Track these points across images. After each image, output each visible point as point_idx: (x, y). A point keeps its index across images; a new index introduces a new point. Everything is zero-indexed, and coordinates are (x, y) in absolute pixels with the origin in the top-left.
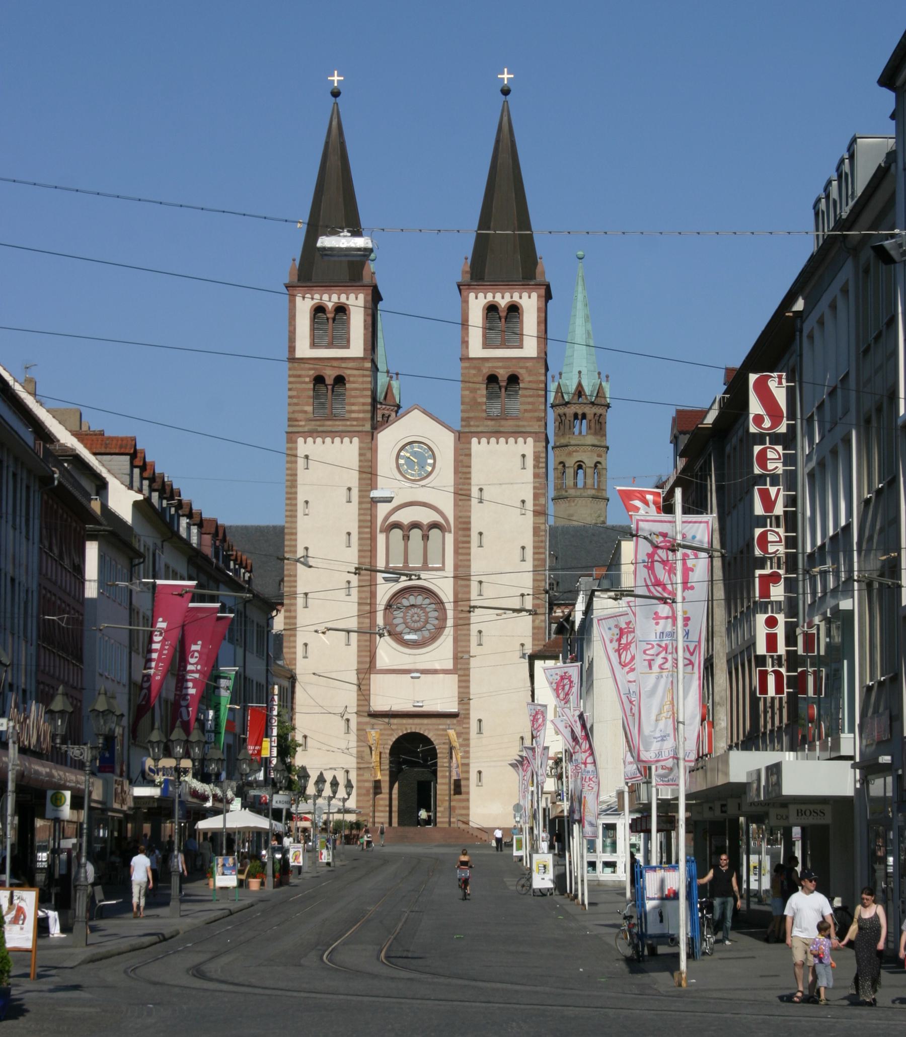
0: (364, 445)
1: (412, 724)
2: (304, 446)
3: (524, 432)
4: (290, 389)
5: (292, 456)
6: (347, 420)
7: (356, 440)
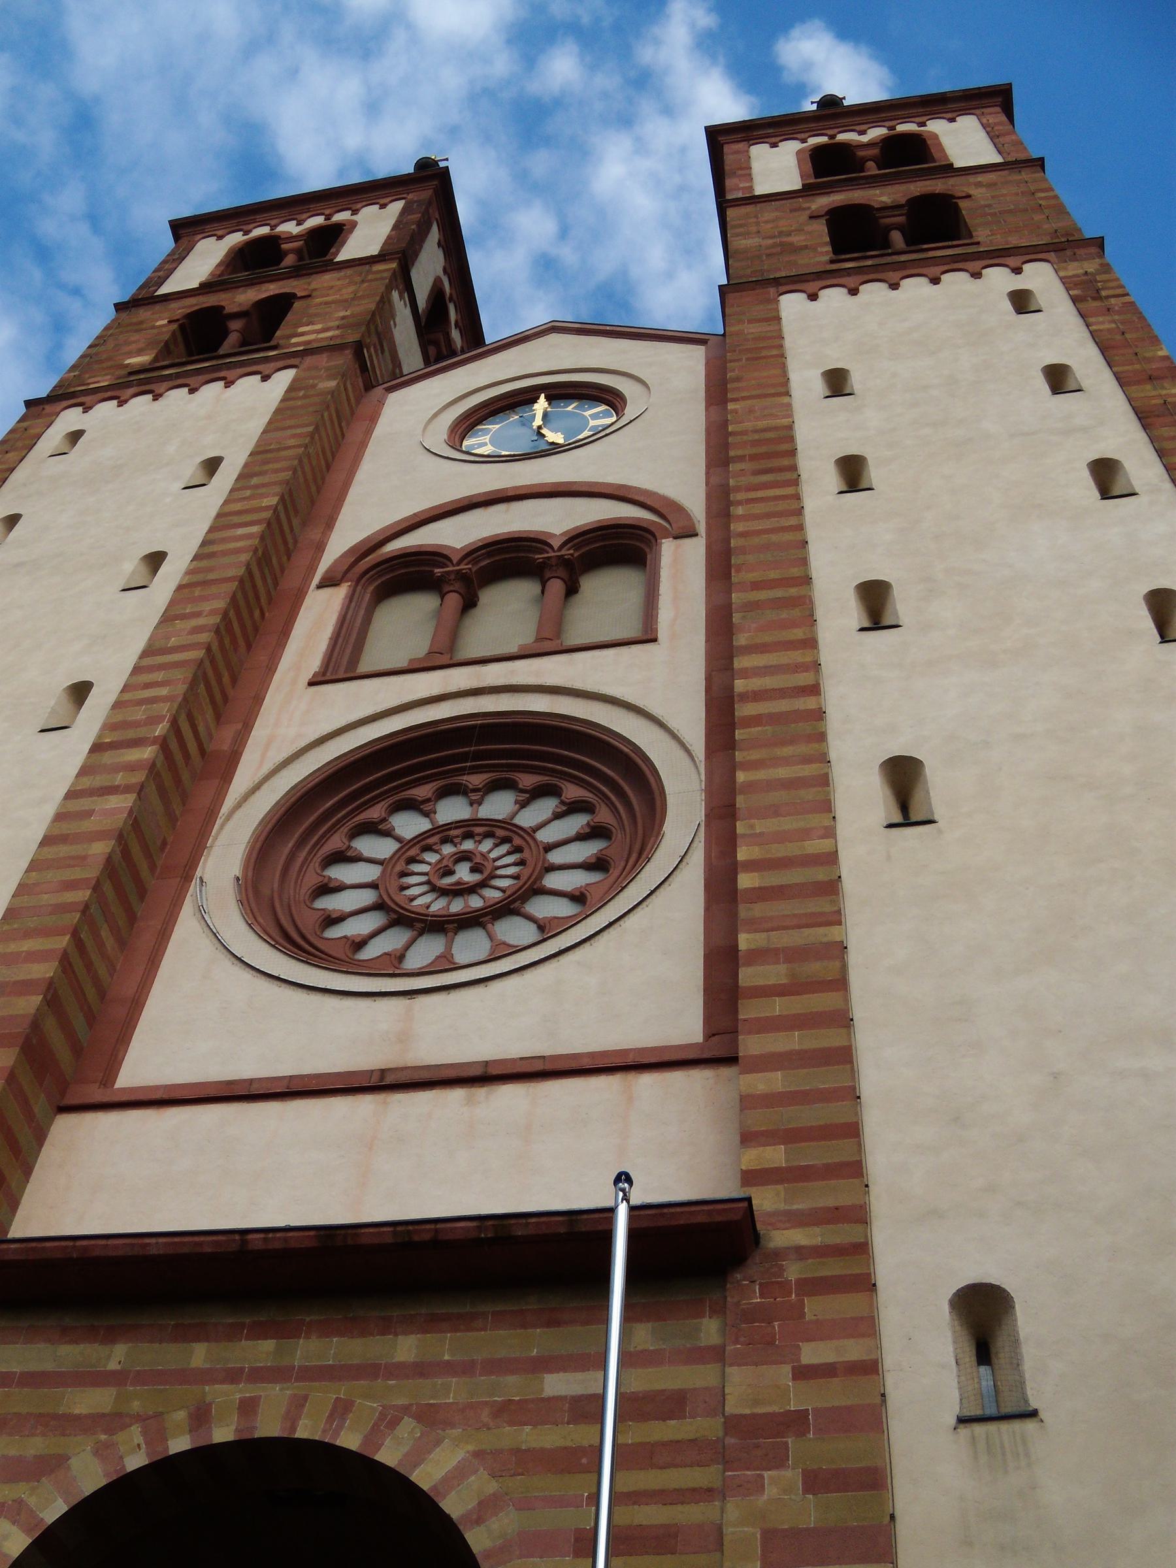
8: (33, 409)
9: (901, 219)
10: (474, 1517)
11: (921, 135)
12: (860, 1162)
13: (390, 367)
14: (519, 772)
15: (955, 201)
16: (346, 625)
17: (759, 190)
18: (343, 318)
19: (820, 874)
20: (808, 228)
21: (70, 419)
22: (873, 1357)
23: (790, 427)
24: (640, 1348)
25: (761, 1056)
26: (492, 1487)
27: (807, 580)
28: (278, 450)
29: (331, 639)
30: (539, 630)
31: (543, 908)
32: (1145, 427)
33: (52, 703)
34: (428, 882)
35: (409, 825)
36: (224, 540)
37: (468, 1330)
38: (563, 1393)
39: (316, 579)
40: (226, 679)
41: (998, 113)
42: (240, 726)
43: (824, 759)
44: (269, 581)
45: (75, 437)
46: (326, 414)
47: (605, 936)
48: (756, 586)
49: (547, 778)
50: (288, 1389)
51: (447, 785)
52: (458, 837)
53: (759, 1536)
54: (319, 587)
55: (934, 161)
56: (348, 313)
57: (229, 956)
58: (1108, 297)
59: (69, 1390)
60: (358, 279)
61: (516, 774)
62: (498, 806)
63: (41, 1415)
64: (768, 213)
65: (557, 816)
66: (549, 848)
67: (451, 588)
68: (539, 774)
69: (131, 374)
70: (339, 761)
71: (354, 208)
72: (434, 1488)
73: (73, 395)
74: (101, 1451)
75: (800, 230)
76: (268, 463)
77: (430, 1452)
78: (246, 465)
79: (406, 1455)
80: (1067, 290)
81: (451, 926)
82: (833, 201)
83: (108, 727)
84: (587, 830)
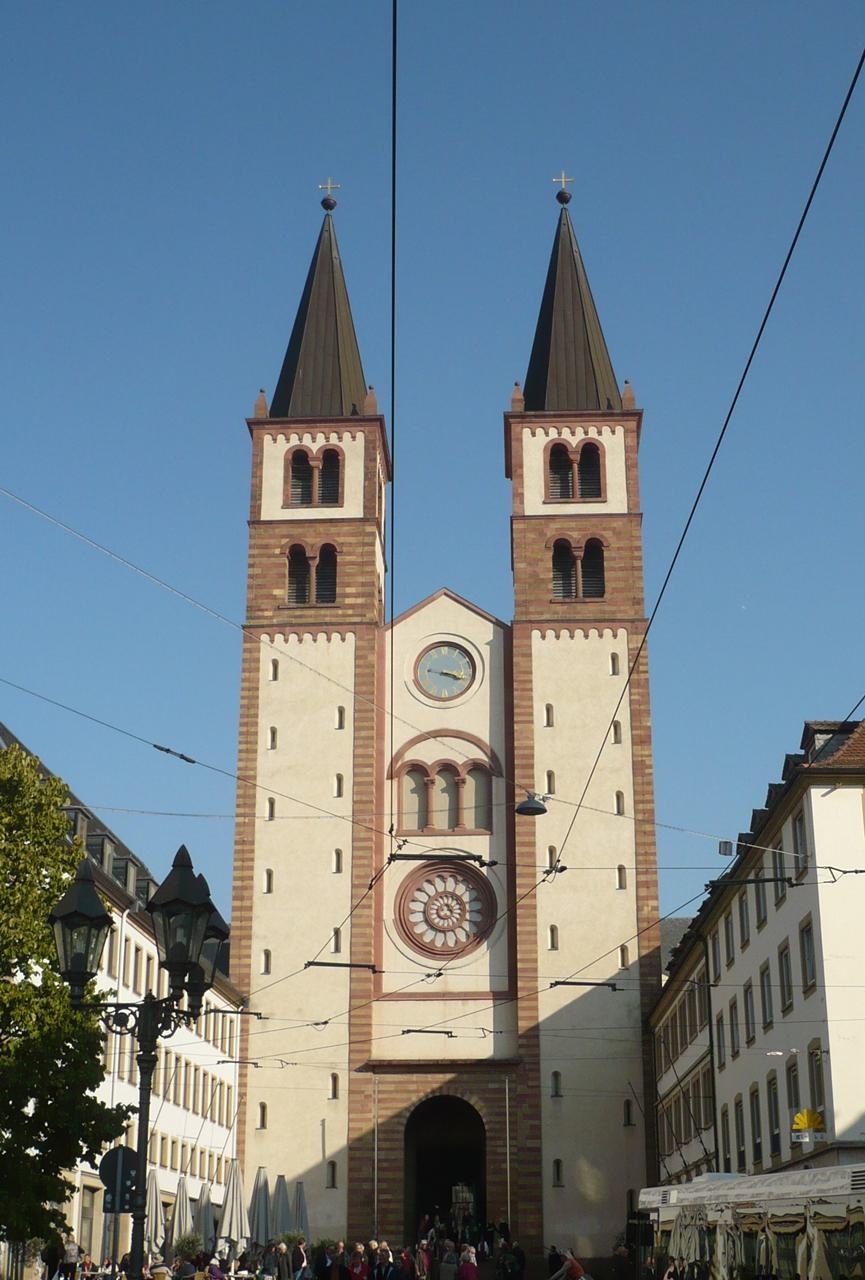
0: (360, 643)
2: (270, 649)
3: (613, 621)
4: (251, 566)
5: (251, 664)
7: (350, 636)
17: (526, 514)
18: (363, 584)
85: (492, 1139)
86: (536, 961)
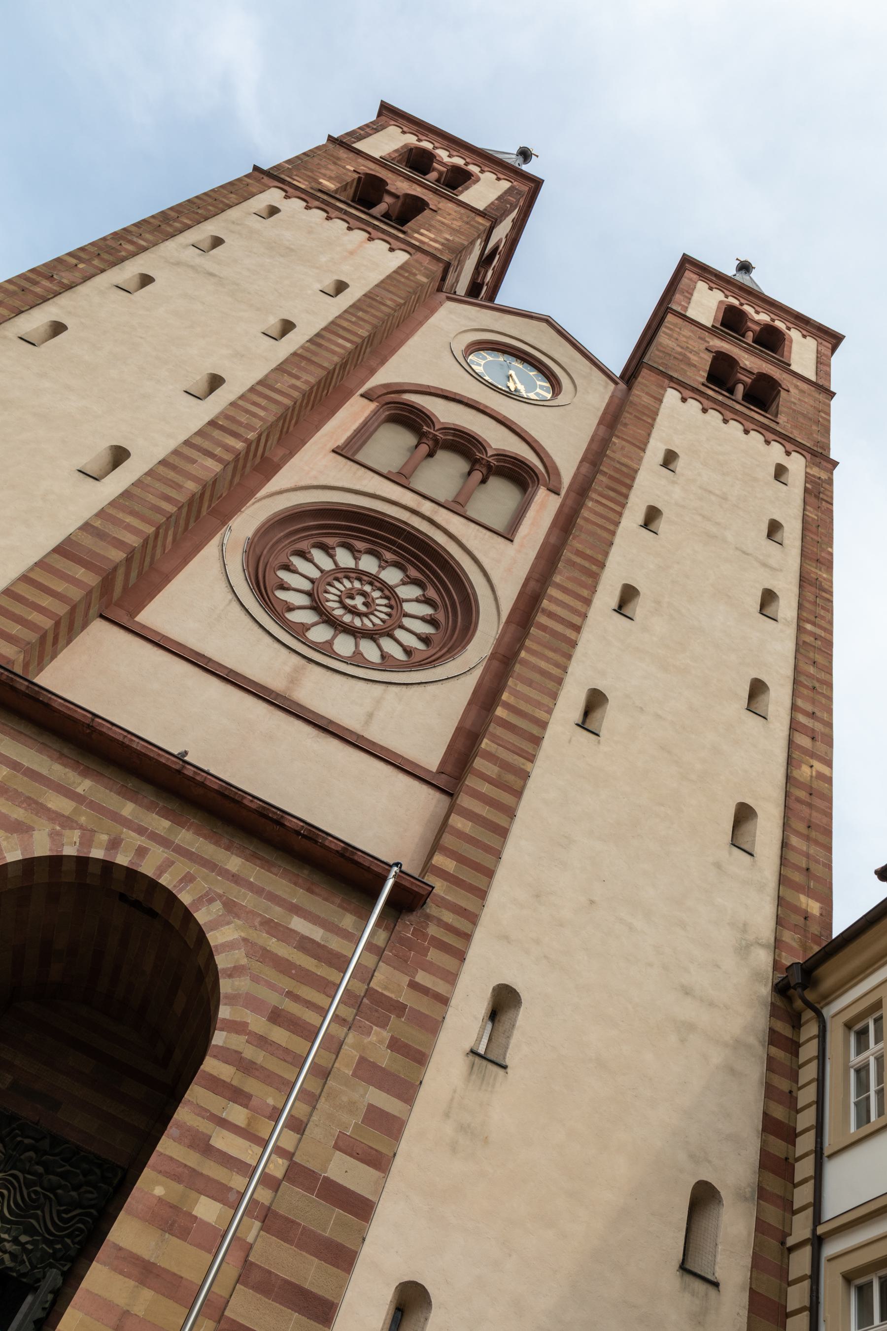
1: (154, 837)
6: (404, 232)
8: (257, 173)
9: (749, 381)
10: (229, 973)
11: (784, 335)
12: (487, 892)
13: (454, 281)
14: (412, 566)
15: (780, 388)
16: (365, 428)
18: (448, 240)
19: (535, 730)
20: (702, 355)
21: (273, 196)
22: (448, 996)
23: (636, 471)
24: (344, 927)
25: (466, 809)
26: (244, 961)
27: (602, 565)
28: (381, 303)
29: (355, 431)
30: (458, 495)
31: (388, 645)
32: (801, 586)
33: (198, 378)
34: (339, 596)
35: (344, 559)
36: (329, 340)
37: (268, 871)
38: (299, 931)
39: (362, 390)
40: (293, 422)
41: (829, 348)
42: (287, 452)
43: (565, 670)
44: (340, 377)
45: (273, 211)
46: (413, 297)
47: (415, 688)
48: (579, 553)
49: (423, 578)
50: (166, 853)
51: (372, 549)
52: (365, 581)
53: (357, 1058)
54: (362, 396)
55: (782, 356)
56: (451, 238)
57: (227, 581)
58: (822, 499)
59: (50, 791)
60: (465, 219)
61: (410, 566)
62: (392, 576)
63: (29, 798)
64: (687, 331)
65: (417, 600)
66: (406, 615)
67: (427, 442)
68: (421, 574)
69: (320, 191)
70: (327, 504)
71: (483, 169)
72: (216, 946)
73: (283, 181)
74: (53, 835)
75: (697, 353)
76: (373, 308)
77: (222, 926)
78: (359, 300)
79: (210, 921)
80: (806, 482)
81: (340, 628)
82: (722, 347)
83: (224, 414)
84: (429, 618)
85: (216, 1085)
86: (544, 725)
